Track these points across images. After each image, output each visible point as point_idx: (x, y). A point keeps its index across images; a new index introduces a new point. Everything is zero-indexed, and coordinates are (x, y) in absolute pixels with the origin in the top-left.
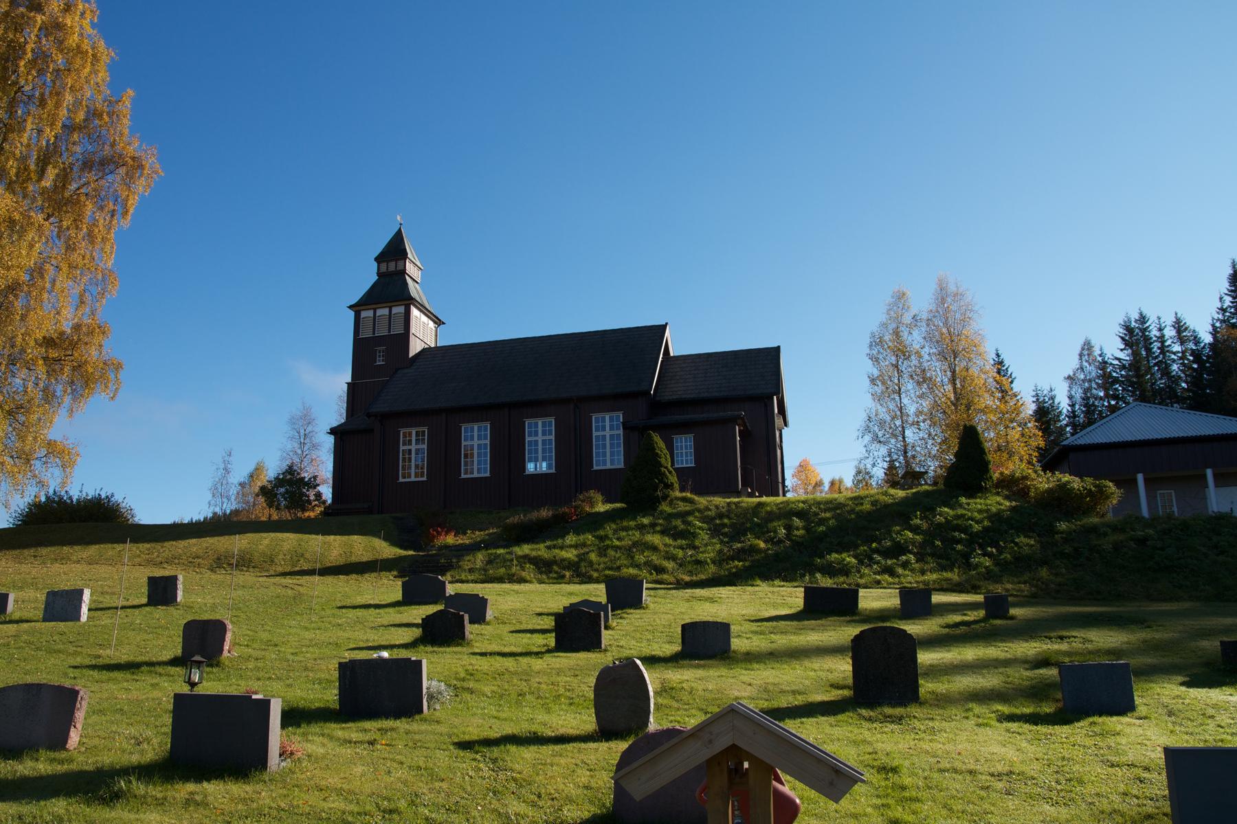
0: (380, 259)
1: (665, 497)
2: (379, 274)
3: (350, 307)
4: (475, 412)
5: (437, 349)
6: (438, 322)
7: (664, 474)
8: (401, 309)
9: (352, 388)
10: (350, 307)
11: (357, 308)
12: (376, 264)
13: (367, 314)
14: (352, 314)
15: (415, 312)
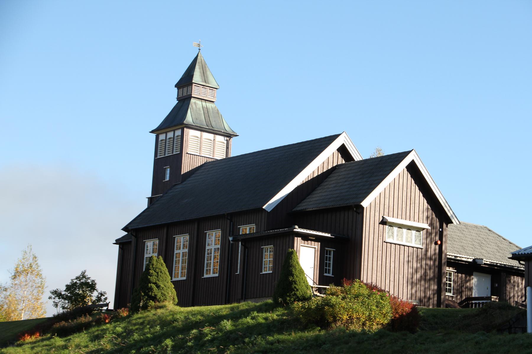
0: (179, 85)
1: (145, 308)
2: (178, 99)
3: (152, 132)
4: (180, 226)
5: (228, 161)
6: (229, 136)
7: (151, 289)
8: (178, 133)
9: (151, 200)
10: (152, 132)
11: (157, 131)
12: (176, 89)
13: (162, 137)
14: (154, 136)
15: (191, 135)
